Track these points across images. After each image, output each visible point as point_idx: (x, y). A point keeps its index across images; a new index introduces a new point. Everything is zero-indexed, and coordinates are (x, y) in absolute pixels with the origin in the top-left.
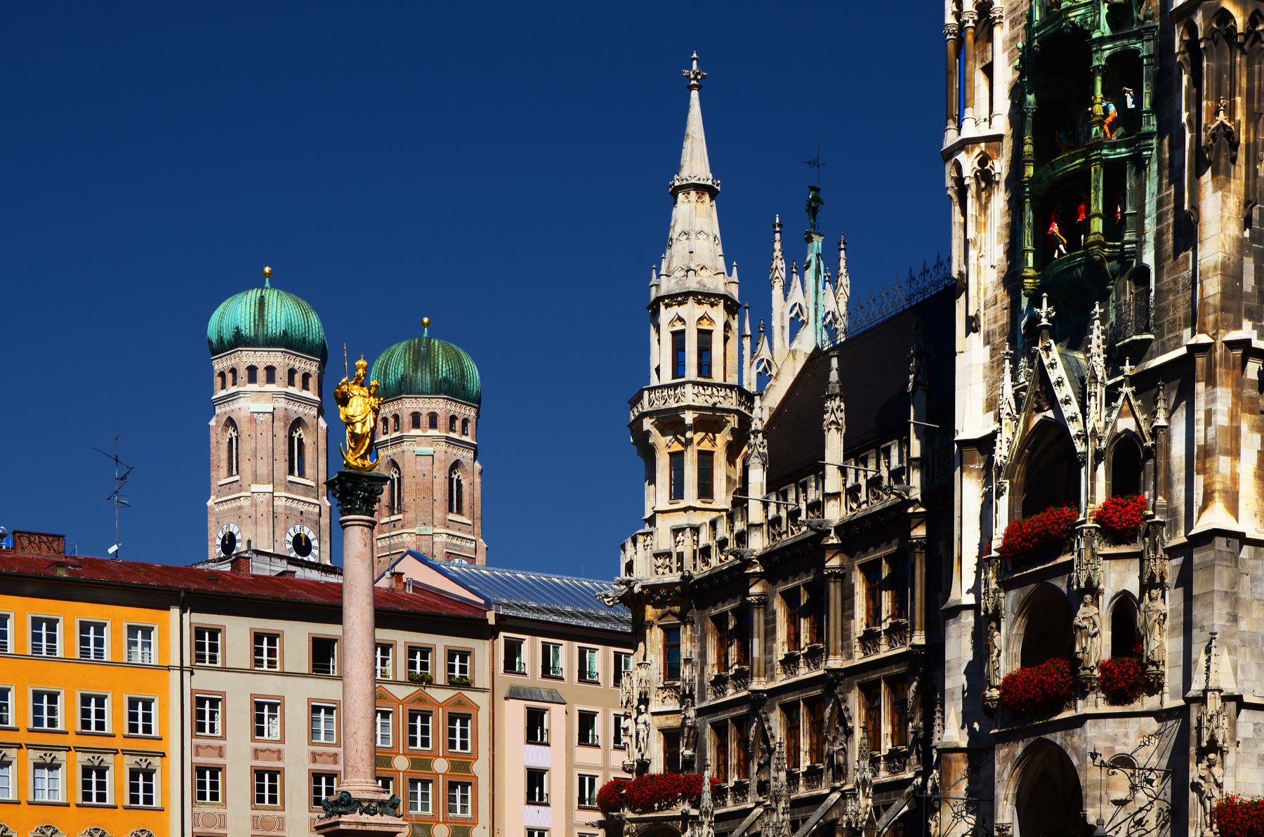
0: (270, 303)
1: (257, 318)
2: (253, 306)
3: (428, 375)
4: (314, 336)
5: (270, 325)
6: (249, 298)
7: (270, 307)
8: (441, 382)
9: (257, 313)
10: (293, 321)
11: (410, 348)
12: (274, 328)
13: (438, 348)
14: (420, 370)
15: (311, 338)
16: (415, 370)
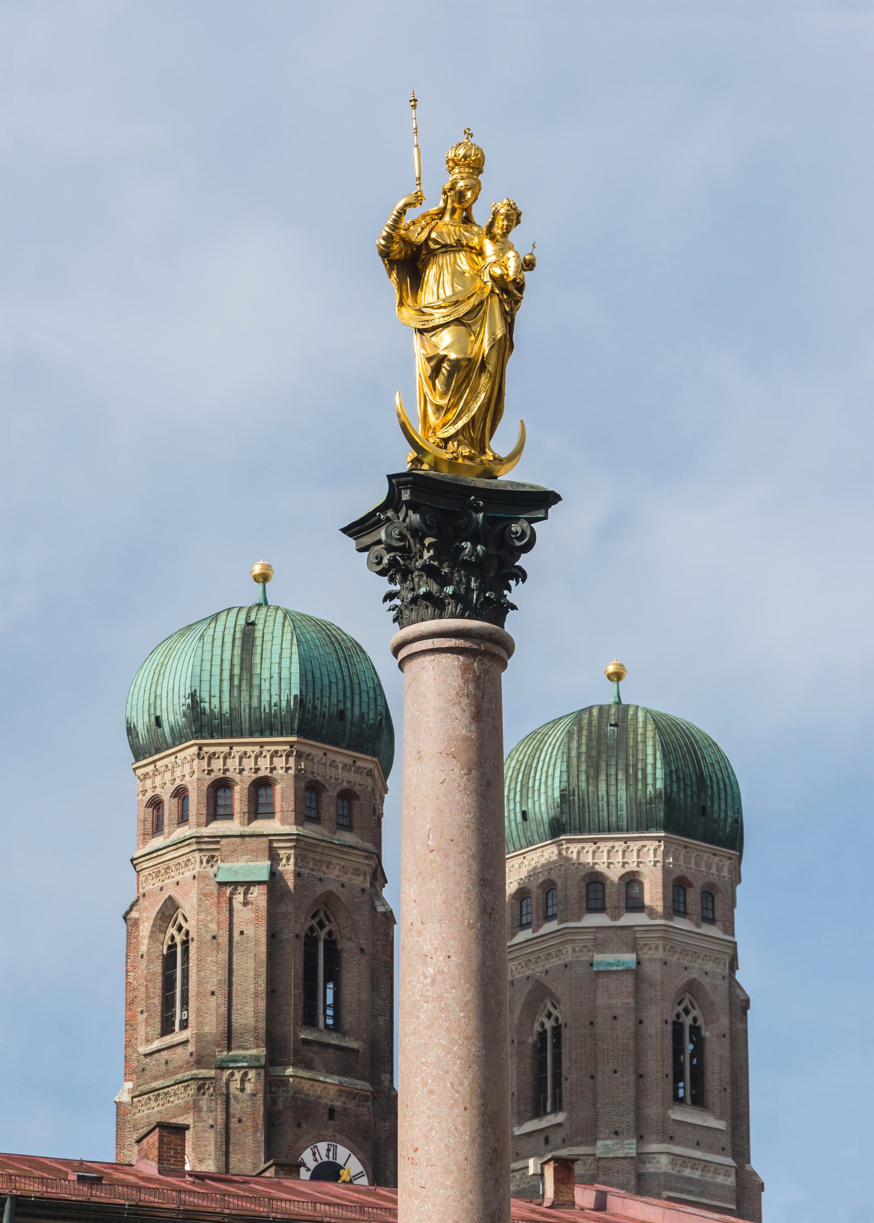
0: (268, 637)
1: (237, 671)
2: (228, 646)
3: (622, 786)
4: (365, 707)
5: (265, 686)
6: (220, 628)
7: (267, 645)
8: (651, 802)
9: (237, 661)
10: (317, 675)
11: (580, 730)
12: (275, 691)
13: (645, 727)
14: (603, 777)
15: (357, 712)
16: (593, 777)
